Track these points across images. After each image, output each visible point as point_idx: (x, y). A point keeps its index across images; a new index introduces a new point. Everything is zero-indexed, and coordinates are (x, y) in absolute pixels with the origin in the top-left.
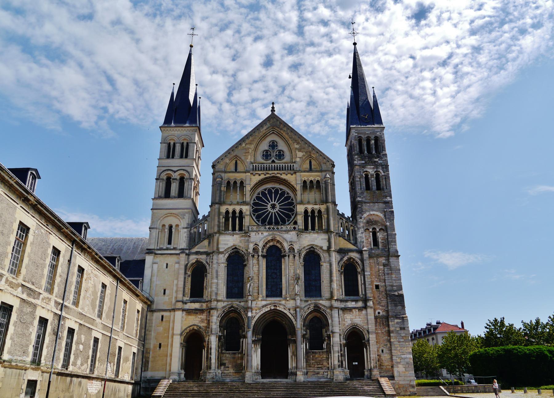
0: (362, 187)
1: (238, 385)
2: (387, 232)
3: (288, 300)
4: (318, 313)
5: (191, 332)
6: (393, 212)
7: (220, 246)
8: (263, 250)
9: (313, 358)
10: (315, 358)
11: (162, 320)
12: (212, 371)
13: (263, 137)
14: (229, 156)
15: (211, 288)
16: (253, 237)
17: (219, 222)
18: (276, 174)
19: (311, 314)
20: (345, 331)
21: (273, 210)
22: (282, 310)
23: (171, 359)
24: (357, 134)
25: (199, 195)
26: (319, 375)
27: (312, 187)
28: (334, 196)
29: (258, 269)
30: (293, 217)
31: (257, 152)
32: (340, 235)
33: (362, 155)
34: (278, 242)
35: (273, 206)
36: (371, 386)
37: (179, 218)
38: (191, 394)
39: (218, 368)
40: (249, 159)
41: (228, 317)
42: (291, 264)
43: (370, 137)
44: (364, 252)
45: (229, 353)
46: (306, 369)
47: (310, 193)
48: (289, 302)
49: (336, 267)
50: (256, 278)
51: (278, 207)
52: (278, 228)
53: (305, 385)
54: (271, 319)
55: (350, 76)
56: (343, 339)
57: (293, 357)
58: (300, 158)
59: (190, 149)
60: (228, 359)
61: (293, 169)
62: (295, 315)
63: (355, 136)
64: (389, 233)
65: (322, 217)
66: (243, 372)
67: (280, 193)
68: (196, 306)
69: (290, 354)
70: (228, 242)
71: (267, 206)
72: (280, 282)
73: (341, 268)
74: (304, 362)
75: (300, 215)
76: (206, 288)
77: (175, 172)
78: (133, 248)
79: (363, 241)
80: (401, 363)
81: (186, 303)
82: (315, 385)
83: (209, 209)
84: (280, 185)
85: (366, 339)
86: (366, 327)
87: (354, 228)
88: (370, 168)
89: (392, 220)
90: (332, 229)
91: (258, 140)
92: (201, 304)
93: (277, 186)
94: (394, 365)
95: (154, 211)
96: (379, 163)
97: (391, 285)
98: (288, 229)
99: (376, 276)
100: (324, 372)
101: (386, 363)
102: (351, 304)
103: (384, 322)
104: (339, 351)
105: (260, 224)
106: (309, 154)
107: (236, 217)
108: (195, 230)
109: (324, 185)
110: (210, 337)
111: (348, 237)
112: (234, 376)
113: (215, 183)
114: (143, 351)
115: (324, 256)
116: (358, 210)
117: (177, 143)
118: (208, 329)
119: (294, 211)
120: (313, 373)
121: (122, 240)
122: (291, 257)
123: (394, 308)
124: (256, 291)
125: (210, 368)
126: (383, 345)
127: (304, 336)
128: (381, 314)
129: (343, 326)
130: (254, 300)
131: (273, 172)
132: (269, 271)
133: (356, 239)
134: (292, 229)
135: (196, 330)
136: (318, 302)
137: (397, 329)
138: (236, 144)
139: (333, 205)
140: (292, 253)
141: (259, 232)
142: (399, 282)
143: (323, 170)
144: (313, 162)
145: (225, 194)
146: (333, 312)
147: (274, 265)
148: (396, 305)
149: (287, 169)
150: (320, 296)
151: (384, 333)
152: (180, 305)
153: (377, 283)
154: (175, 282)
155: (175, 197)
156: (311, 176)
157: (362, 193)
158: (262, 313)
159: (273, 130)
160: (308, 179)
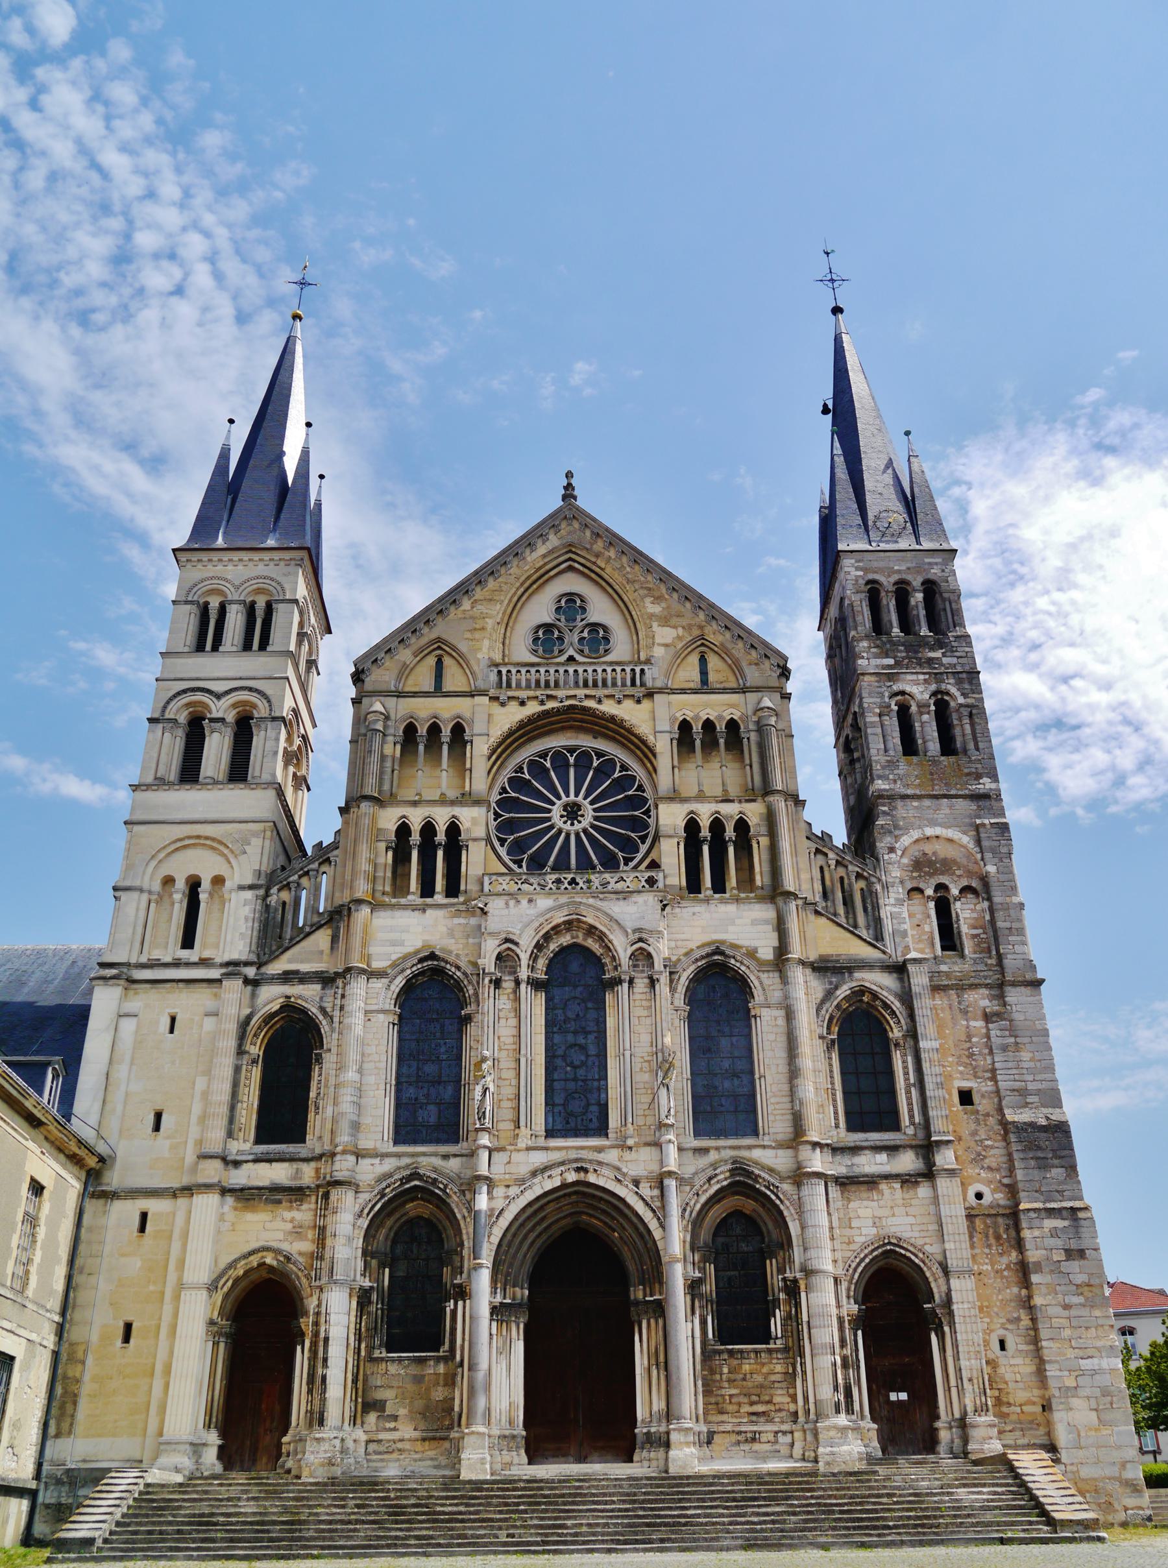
0: (890, 745)
1: (427, 1490)
2: (989, 899)
3: (630, 1148)
4: (748, 1197)
5: (254, 1277)
6: (1004, 828)
9: (732, 1376)
11: (142, 1229)
12: (326, 1433)
13: (534, 582)
14: (413, 640)
16: (496, 912)
19: (719, 1201)
20: (853, 1265)
21: (572, 824)
22: (607, 1186)
23: (167, 1386)
24: (861, 573)
25: (309, 789)
26: (756, 1446)
27: (710, 744)
28: (790, 771)
29: (514, 1032)
30: (643, 848)
31: (512, 629)
32: (819, 909)
34: (591, 930)
35: (573, 812)
36: (984, 1485)
37: (226, 851)
38: (227, 1531)
39: (354, 1421)
40: (485, 650)
41: (397, 1215)
42: (638, 1012)
43: (908, 583)
44: (911, 968)
45: (400, 1360)
46: (706, 1422)
47: (706, 765)
48: (633, 1155)
49: (809, 1023)
50: (507, 1063)
51: (591, 813)
53: (705, 1485)
54: (564, 1222)
55: (825, 405)
56: (848, 1297)
57: (654, 1372)
58: (666, 645)
59: (278, 620)
60: (395, 1384)
61: (643, 684)
62: (658, 1204)
64: (997, 899)
65: (750, 847)
66: (453, 1435)
67: (595, 764)
68: (279, 1173)
69: (640, 1361)
71: (549, 811)
72: (599, 1080)
73: (829, 1028)
75: (670, 836)
77: (219, 696)
78: (64, 979)
79: (905, 931)
80: (1081, 1392)
81: (237, 1164)
82: (751, 1483)
83: (337, 822)
84: (595, 738)
85: (937, 1297)
86: (933, 1249)
87: (870, 884)
89: (1005, 857)
90: (789, 884)
92: (295, 1165)
93: (586, 742)
94: (1054, 1401)
95: (136, 828)
96: (942, 665)
97: (1017, 1090)
98: (628, 883)
99: (960, 1057)
100: (776, 1433)
101: (1022, 1393)
102: (871, 1164)
103: (1001, 1230)
106: (696, 632)
107: (435, 848)
108: (285, 896)
109: (753, 736)
110: (324, 1296)
111: (847, 918)
113: (363, 731)
114: (56, 1355)
115: (763, 985)
116: (880, 822)
117: (231, 602)
119: (647, 826)
120: (734, 1438)
121: (28, 952)
122: (641, 984)
123: (1036, 1174)
124: (507, 1113)
125: (321, 1422)
126: (1004, 1320)
127: (693, 1287)
128: (987, 1199)
129: (845, 1246)
131: (572, 693)
132: (557, 1038)
133: (877, 924)
134: (644, 883)
135: (271, 1267)
136: (745, 1154)
137: (1056, 1258)
138: (441, 600)
139: (791, 803)
140: (643, 971)
142: (1048, 1076)
143: (748, 684)
144: (713, 662)
145: (396, 767)
146: (805, 1191)
147: (578, 1015)
148: (1043, 1165)
150: (755, 1133)
151: (1006, 1273)
152: (212, 1171)
153: (966, 1084)
154: (201, 1084)
155: (216, 782)
157: (892, 764)
158: (530, 1196)
159: (570, 559)
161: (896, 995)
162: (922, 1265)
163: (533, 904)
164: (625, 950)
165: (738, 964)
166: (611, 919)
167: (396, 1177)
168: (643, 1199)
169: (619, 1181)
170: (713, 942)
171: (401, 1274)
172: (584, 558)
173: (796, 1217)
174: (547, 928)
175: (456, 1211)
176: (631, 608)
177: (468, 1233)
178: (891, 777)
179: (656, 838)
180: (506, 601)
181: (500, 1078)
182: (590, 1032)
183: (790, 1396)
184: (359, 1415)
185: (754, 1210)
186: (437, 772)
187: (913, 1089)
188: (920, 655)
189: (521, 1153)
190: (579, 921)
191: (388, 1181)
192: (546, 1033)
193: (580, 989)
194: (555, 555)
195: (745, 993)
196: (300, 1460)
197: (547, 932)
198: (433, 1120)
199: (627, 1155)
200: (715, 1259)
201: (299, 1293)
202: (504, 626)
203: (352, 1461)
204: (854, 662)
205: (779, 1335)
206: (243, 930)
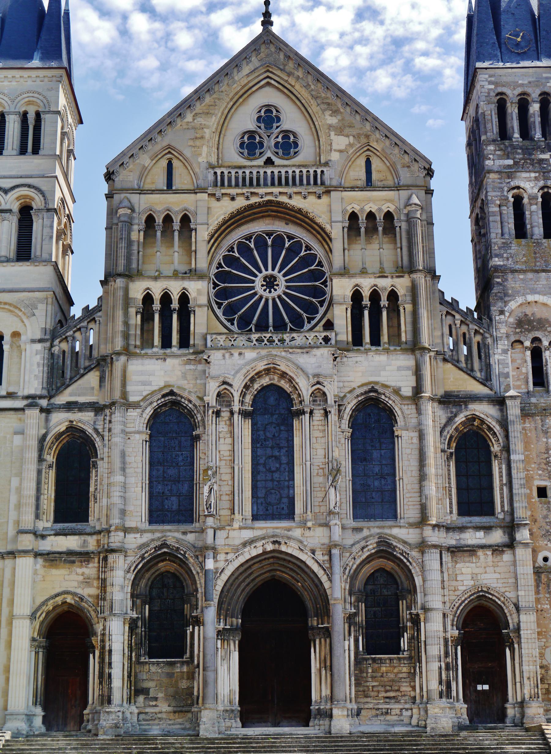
0: (506, 230)
1: (180, 743)
3: (309, 528)
4: (389, 559)
5: (59, 610)
7: (129, 388)
8: (244, 397)
9: (374, 674)
10: (380, 674)
12: (113, 708)
14: (150, 147)
15: (108, 497)
17: (126, 324)
18: (276, 196)
19: (369, 562)
20: (457, 605)
21: (270, 292)
22: (294, 554)
24: (492, 87)
25: (72, 253)
26: (388, 717)
27: (372, 230)
28: (430, 253)
29: (230, 447)
30: (322, 310)
32: (447, 357)
33: (507, 143)
34: (283, 375)
35: (270, 283)
36: (524, 744)
37: (20, 314)
39: (129, 701)
40: (204, 154)
41: (153, 571)
42: (316, 434)
43: (528, 95)
44: (508, 402)
45: (158, 663)
47: (369, 247)
48: (312, 533)
49: (435, 442)
50: (225, 470)
51: (284, 283)
52: (282, 341)
53: (352, 741)
56: (452, 625)
57: (323, 672)
58: (341, 151)
60: (155, 678)
61: (323, 183)
62: (328, 565)
63: (489, 93)
65: (399, 311)
66: (194, 709)
67: (287, 245)
69: (315, 665)
70: (151, 378)
71: (253, 282)
72: (289, 481)
73: (449, 444)
74: (350, 686)
76: (95, 498)
79: (508, 373)
81: (43, 537)
82: (380, 741)
83: (99, 291)
84: (287, 224)
85: (511, 626)
86: (511, 595)
87: (484, 338)
88: (529, 180)
90: (425, 340)
91: (228, 104)
92: (83, 538)
98: (310, 341)
99: (540, 464)
100: (402, 709)
104: (442, 656)
105: (235, 328)
106: (364, 140)
107: (171, 312)
108: (64, 346)
109: (404, 225)
110: (107, 624)
111: (466, 363)
112: (170, 720)
113: (115, 221)
116: (495, 290)
117: (9, 113)
118: (101, 603)
119: (324, 293)
120: (374, 712)
122: (318, 414)
124: (225, 504)
125: (109, 702)
127: (350, 619)
129: (451, 593)
130: (222, 528)
132: (260, 452)
133: (487, 367)
134: (321, 341)
135: (70, 604)
136: (387, 531)
138: (170, 114)
139: (429, 279)
140: (319, 405)
141: (233, 351)
143: (401, 183)
144: (376, 164)
145: (141, 249)
146: (427, 557)
147: (274, 436)
149: (305, 182)
150: (395, 516)
153: (542, 483)
154: (15, 482)
156: (369, 200)
159: (268, 77)
160: (362, 210)
161: (498, 421)
162: (502, 605)
163: (242, 356)
164: (308, 390)
165: (387, 399)
166: (298, 367)
167: (152, 546)
168: (318, 562)
169: (302, 550)
170: (370, 383)
171: (156, 608)
172: (279, 76)
173: (420, 573)
174: (253, 374)
175: (192, 568)
176: (314, 119)
177: (200, 583)
178: (505, 255)
179: (330, 304)
180: (220, 114)
181: (221, 480)
182: (282, 448)
183: (411, 687)
184: (132, 697)
185: (392, 568)
186: (171, 252)
187: (505, 488)
188: (533, 157)
189: (235, 531)
190: (275, 368)
191: (146, 549)
192: (252, 447)
193: (276, 416)
194: (256, 74)
195: (392, 419)
196: (97, 725)
197: (253, 377)
198: (175, 507)
199: (307, 533)
200: (365, 600)
201: (90, 621)
202: (218, 133)
203: (129, 725)
204: (483, 161)
205: (406, 649)
206: (37, 373)
